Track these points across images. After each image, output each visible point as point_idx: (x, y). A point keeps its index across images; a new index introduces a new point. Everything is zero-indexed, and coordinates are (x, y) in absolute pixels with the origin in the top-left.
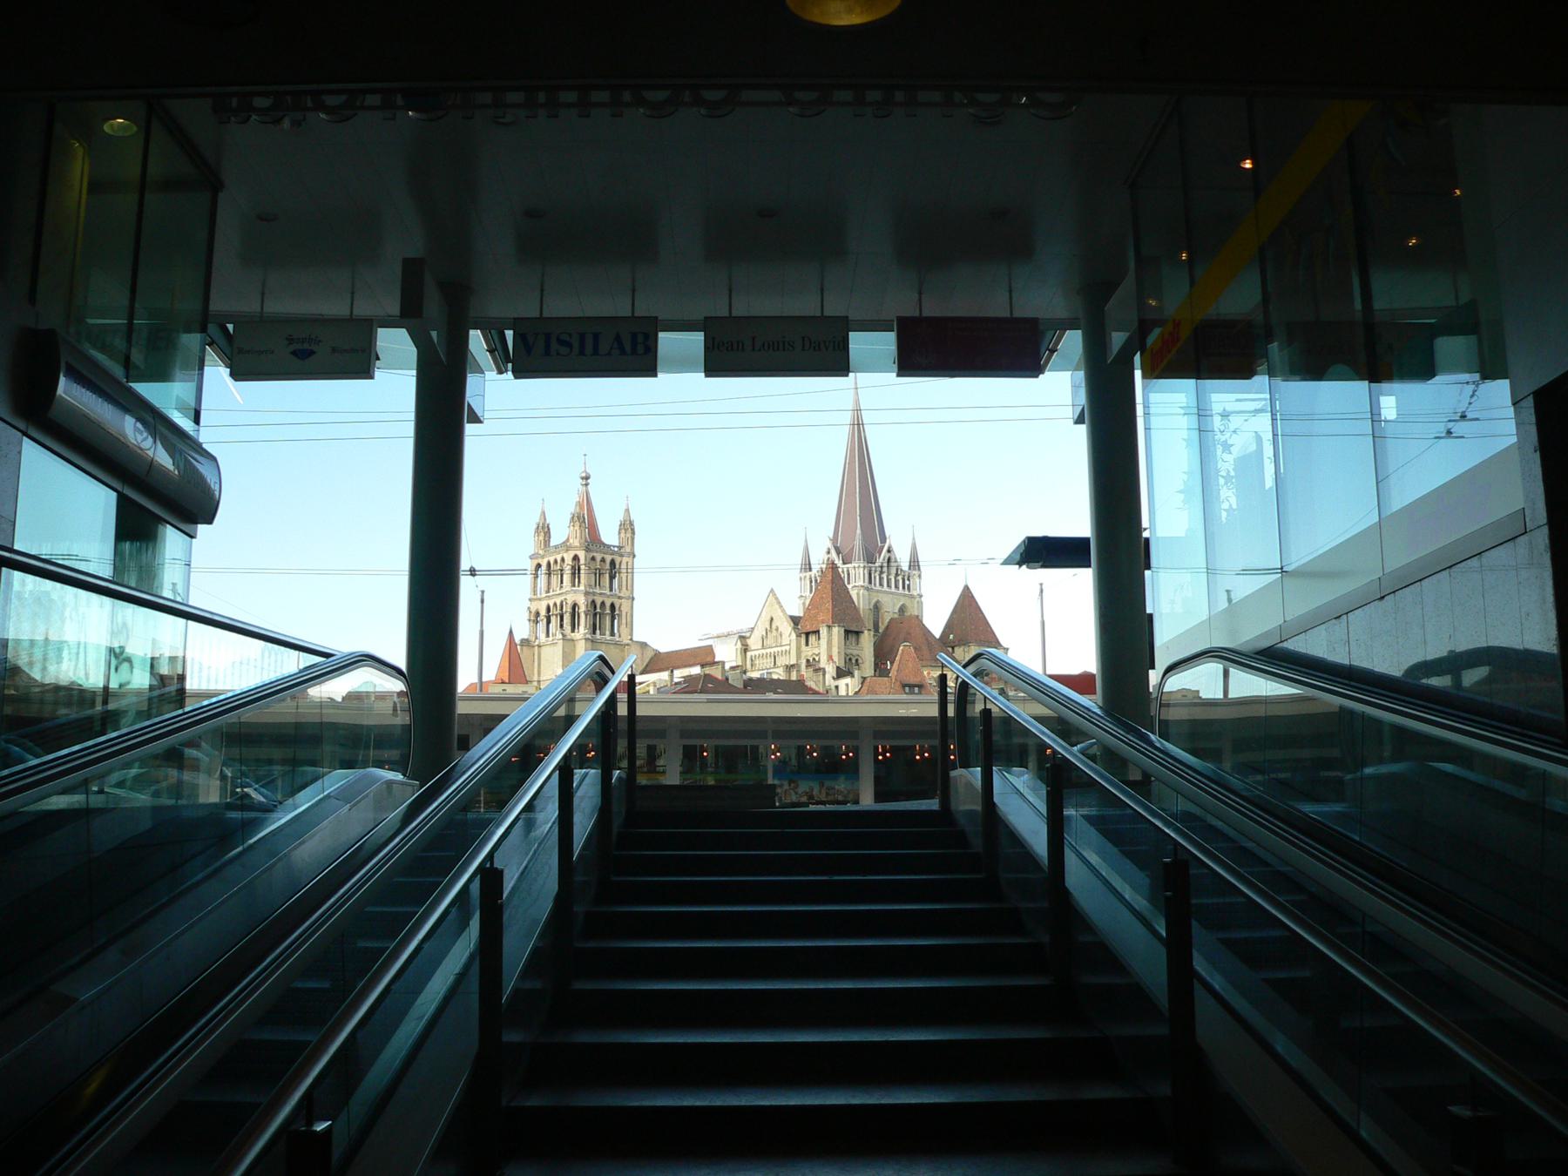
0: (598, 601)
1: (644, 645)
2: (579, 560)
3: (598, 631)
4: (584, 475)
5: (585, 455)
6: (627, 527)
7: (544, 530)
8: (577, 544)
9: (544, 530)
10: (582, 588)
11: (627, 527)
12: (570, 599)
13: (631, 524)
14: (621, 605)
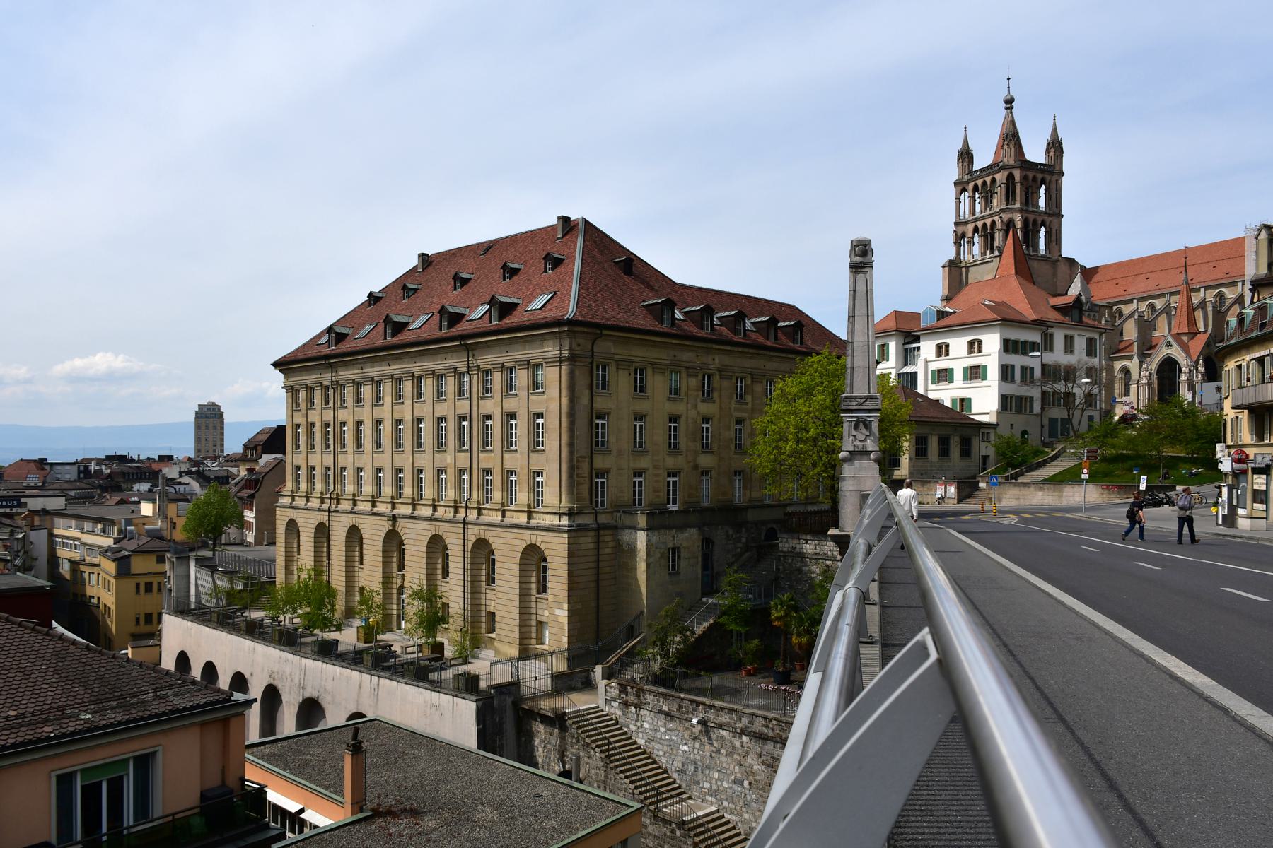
0: (1031, 217)
1: (1072, 262)
2: (1014, 179)
3: (1031, 249)
4: (1009, 97)
5: (1009, 79)
6: (1055, 146)
7: (966, 156)
8: (1012, 162)
9: (966, 156)
10: (1018, 205)
11: (1055, 146)
12: (1006, 217)
13: (1060, 144)
14: (1051, 222)
